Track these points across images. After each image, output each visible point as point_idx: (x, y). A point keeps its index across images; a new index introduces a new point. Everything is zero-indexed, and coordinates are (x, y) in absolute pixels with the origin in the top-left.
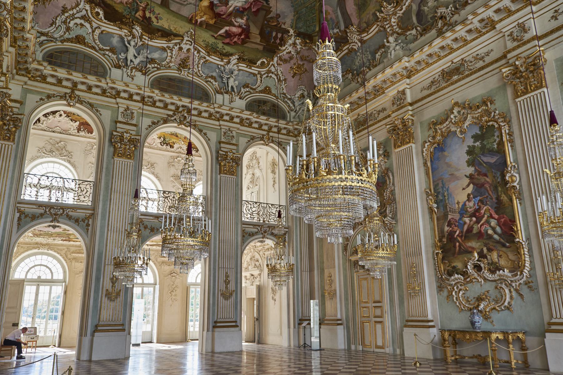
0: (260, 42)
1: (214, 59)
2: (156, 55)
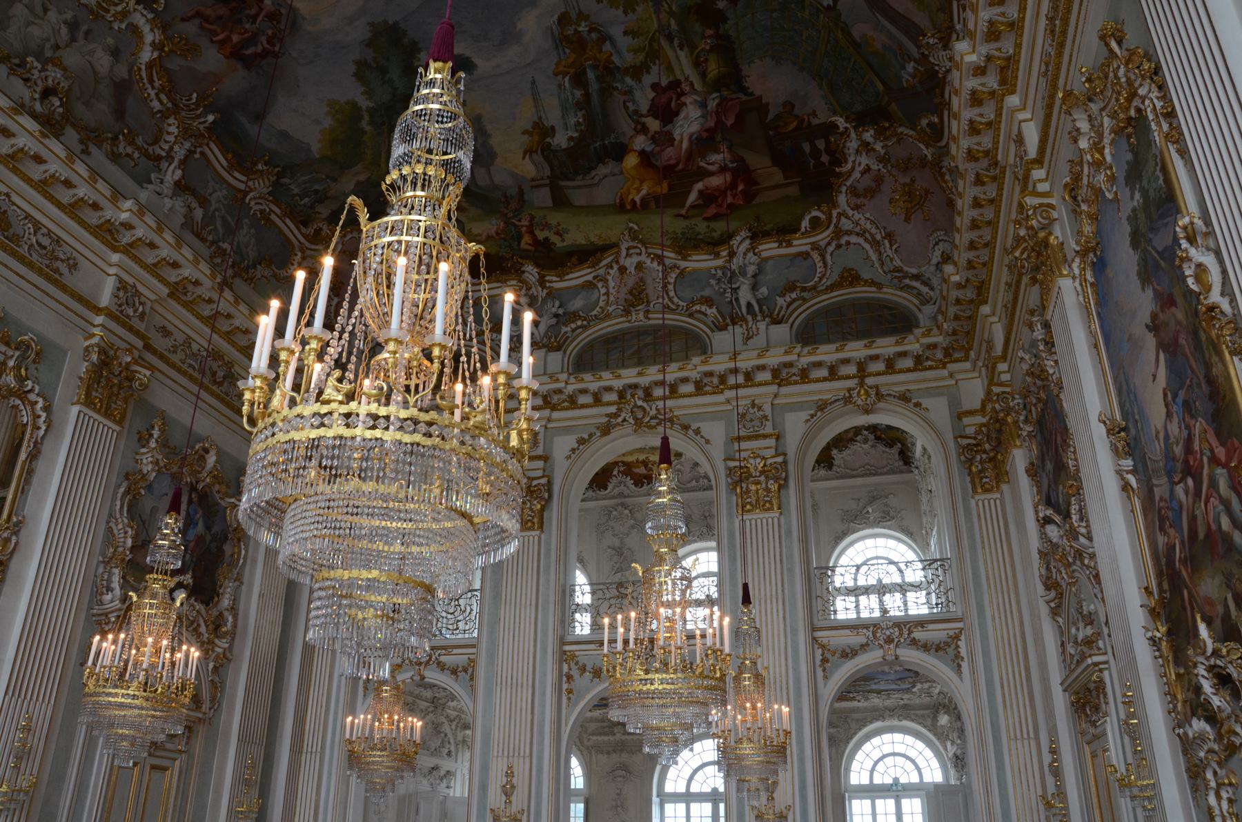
0: (786, 177)
1: (700, 262)
2: (577, 304)
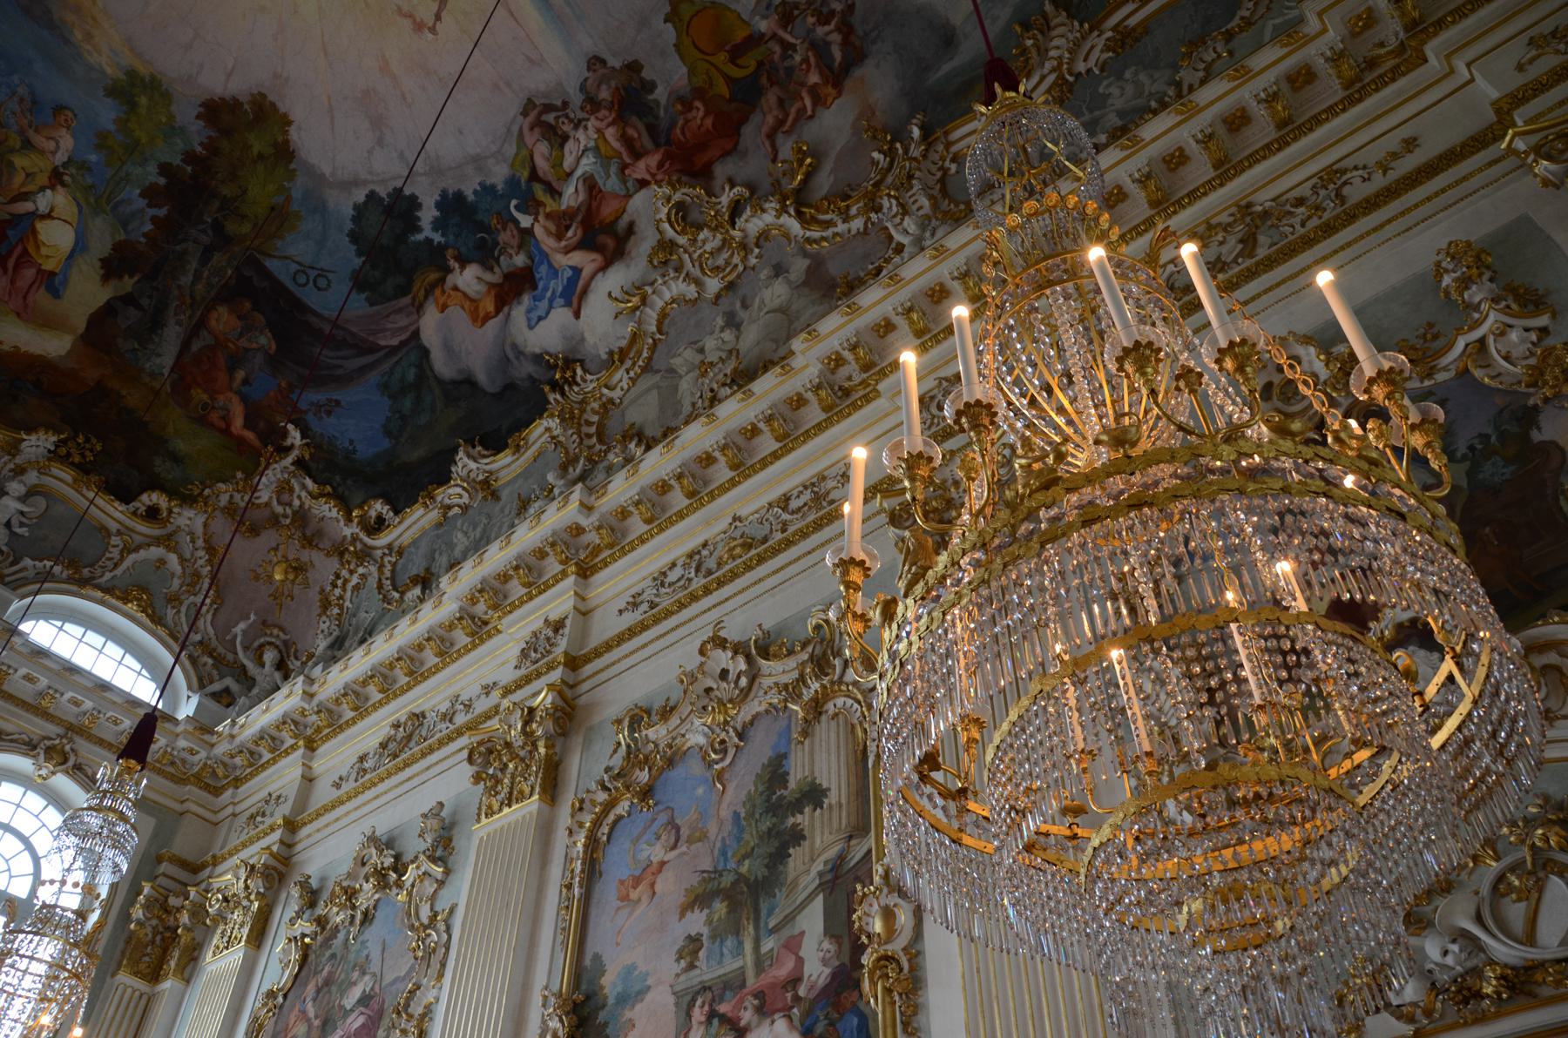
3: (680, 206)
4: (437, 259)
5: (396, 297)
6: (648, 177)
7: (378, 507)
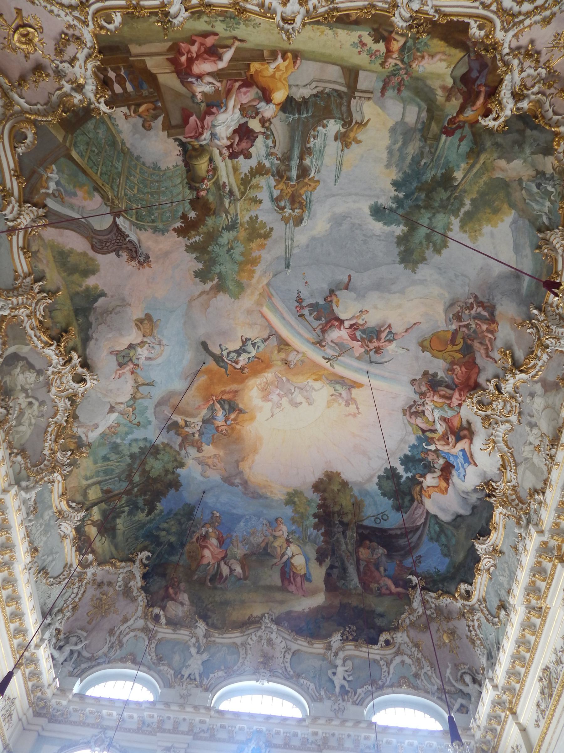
0: (144, 61)
3: (479, 402)
4: (414, 482)
5: (411, 505)
6: (460, 402)
7: (463, 587)
